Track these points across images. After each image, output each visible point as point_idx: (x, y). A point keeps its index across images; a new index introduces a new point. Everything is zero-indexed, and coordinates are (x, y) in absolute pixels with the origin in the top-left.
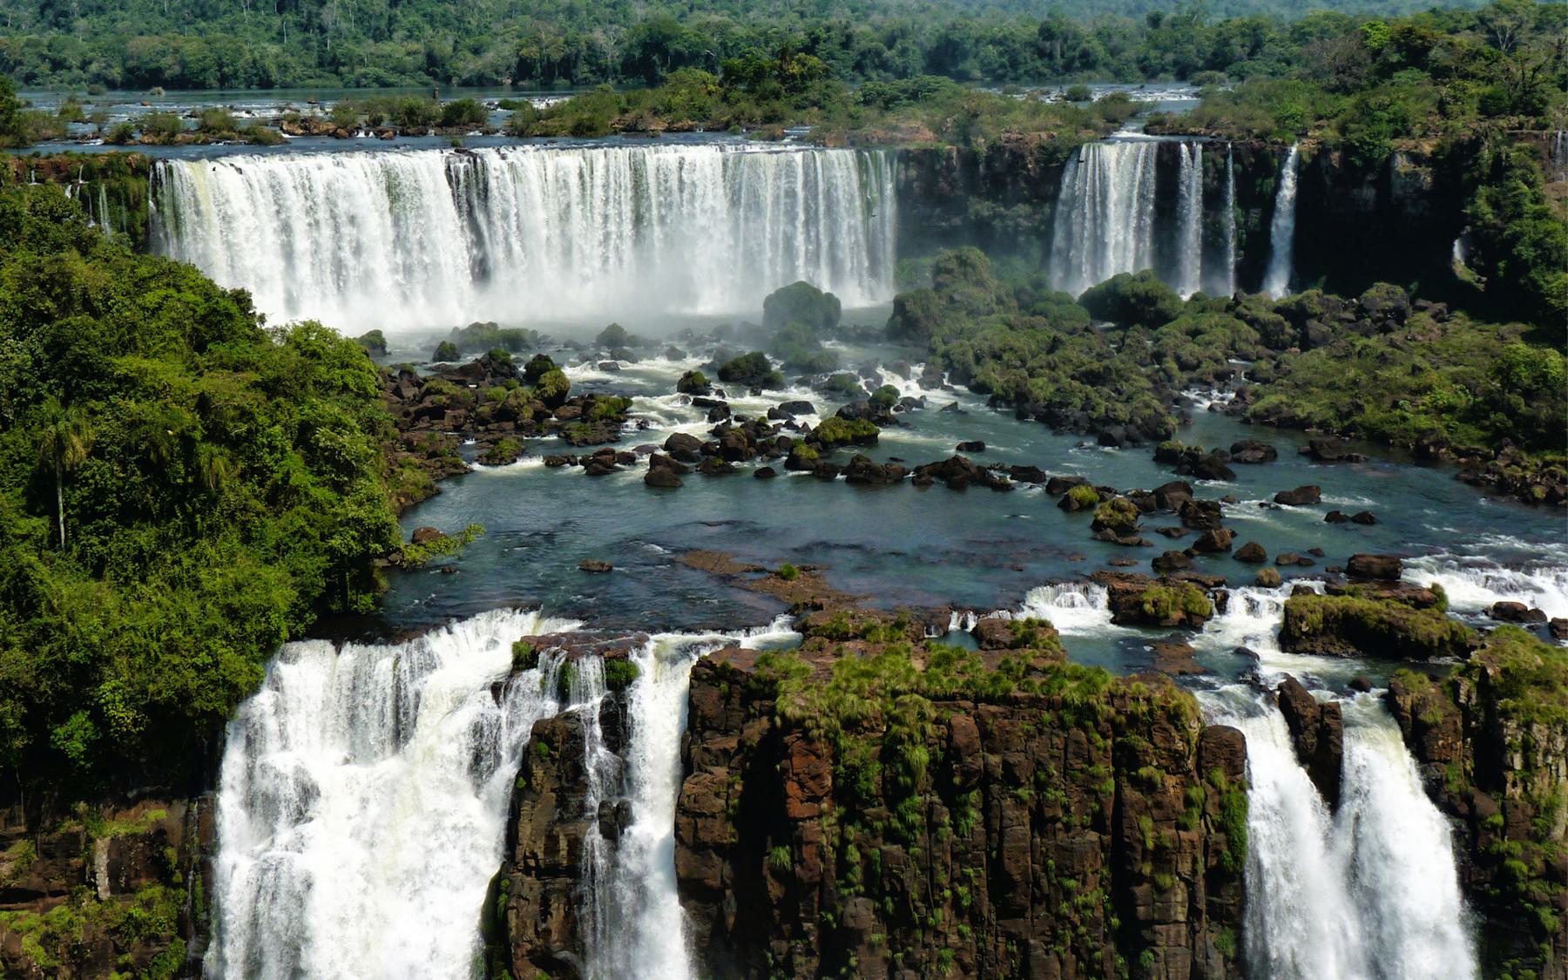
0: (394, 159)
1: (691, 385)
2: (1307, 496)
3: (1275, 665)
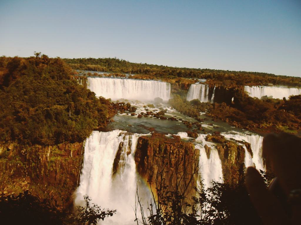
0: (114, 79)
1: (145, 107)
2: (211, 125)
3: (205, 143)
